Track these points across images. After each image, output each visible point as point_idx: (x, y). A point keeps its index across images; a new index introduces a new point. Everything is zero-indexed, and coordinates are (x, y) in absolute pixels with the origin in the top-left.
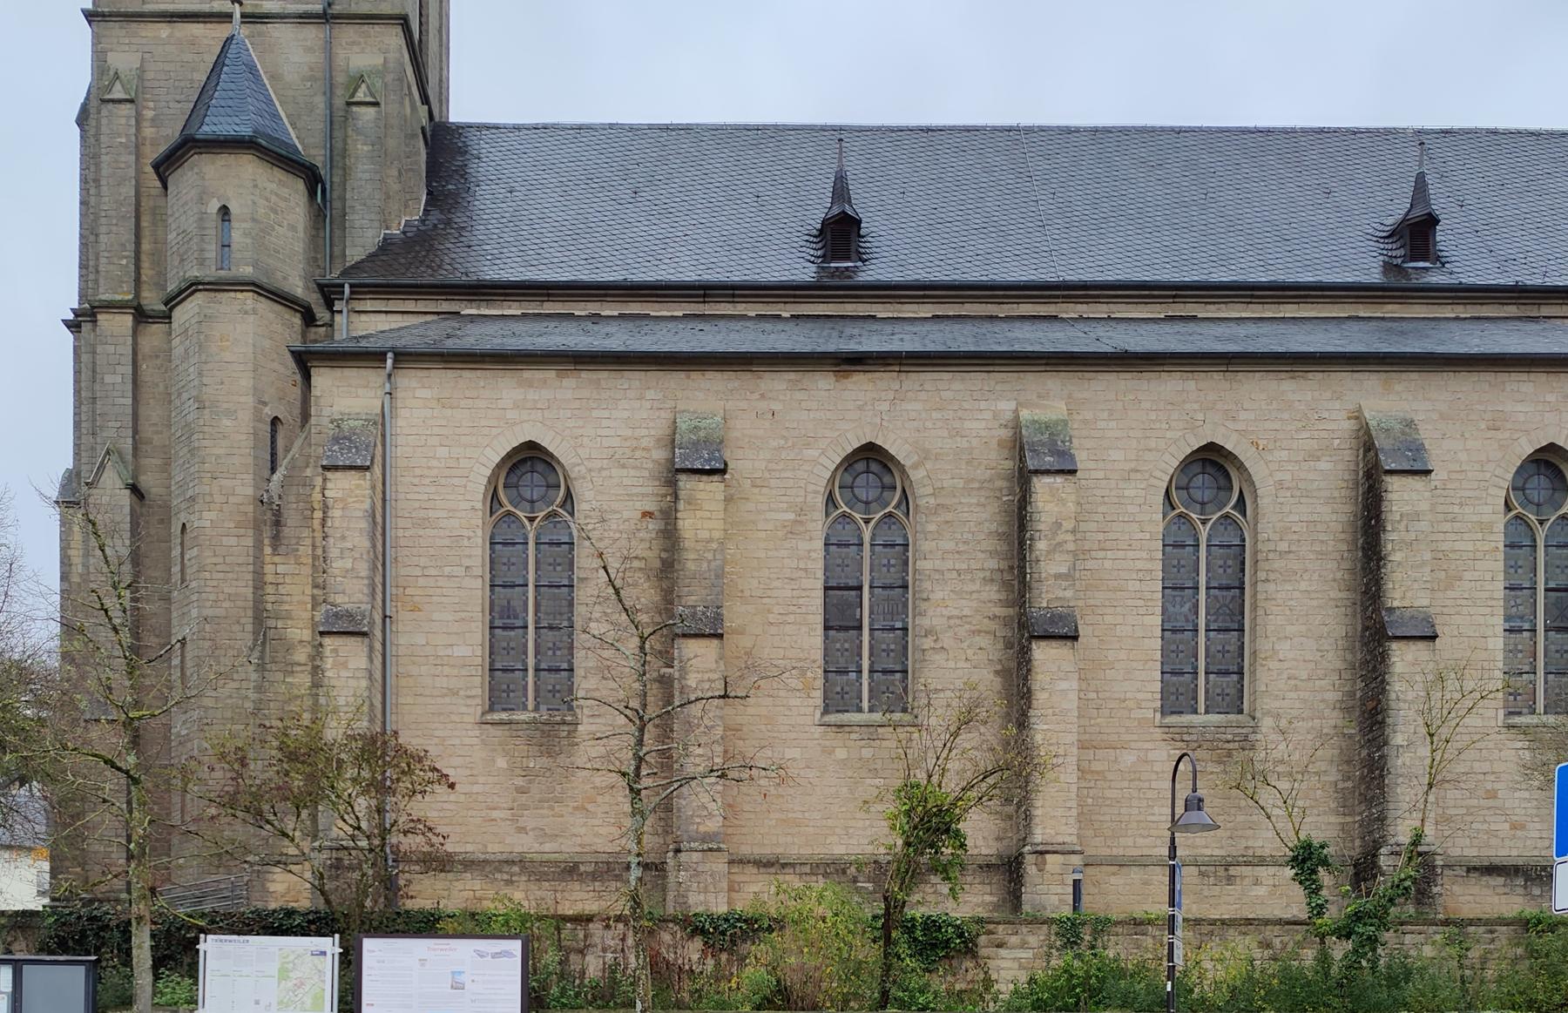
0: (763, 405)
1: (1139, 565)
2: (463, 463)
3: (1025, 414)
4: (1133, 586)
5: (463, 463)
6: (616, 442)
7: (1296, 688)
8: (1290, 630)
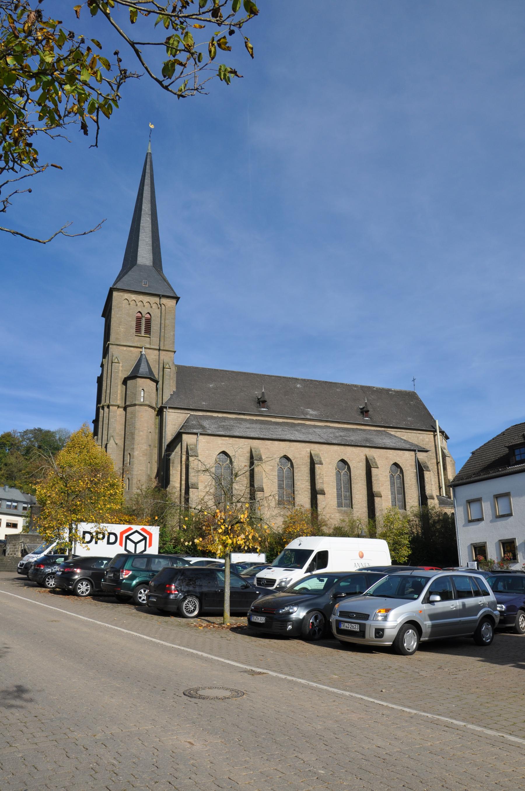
0: (266, 447)
1: (332, 480)
2: (211, 454)
3: (312, 452)
4: (331, 484)
5: (211, 454)
7: (359, 504)
8: (358, 493)
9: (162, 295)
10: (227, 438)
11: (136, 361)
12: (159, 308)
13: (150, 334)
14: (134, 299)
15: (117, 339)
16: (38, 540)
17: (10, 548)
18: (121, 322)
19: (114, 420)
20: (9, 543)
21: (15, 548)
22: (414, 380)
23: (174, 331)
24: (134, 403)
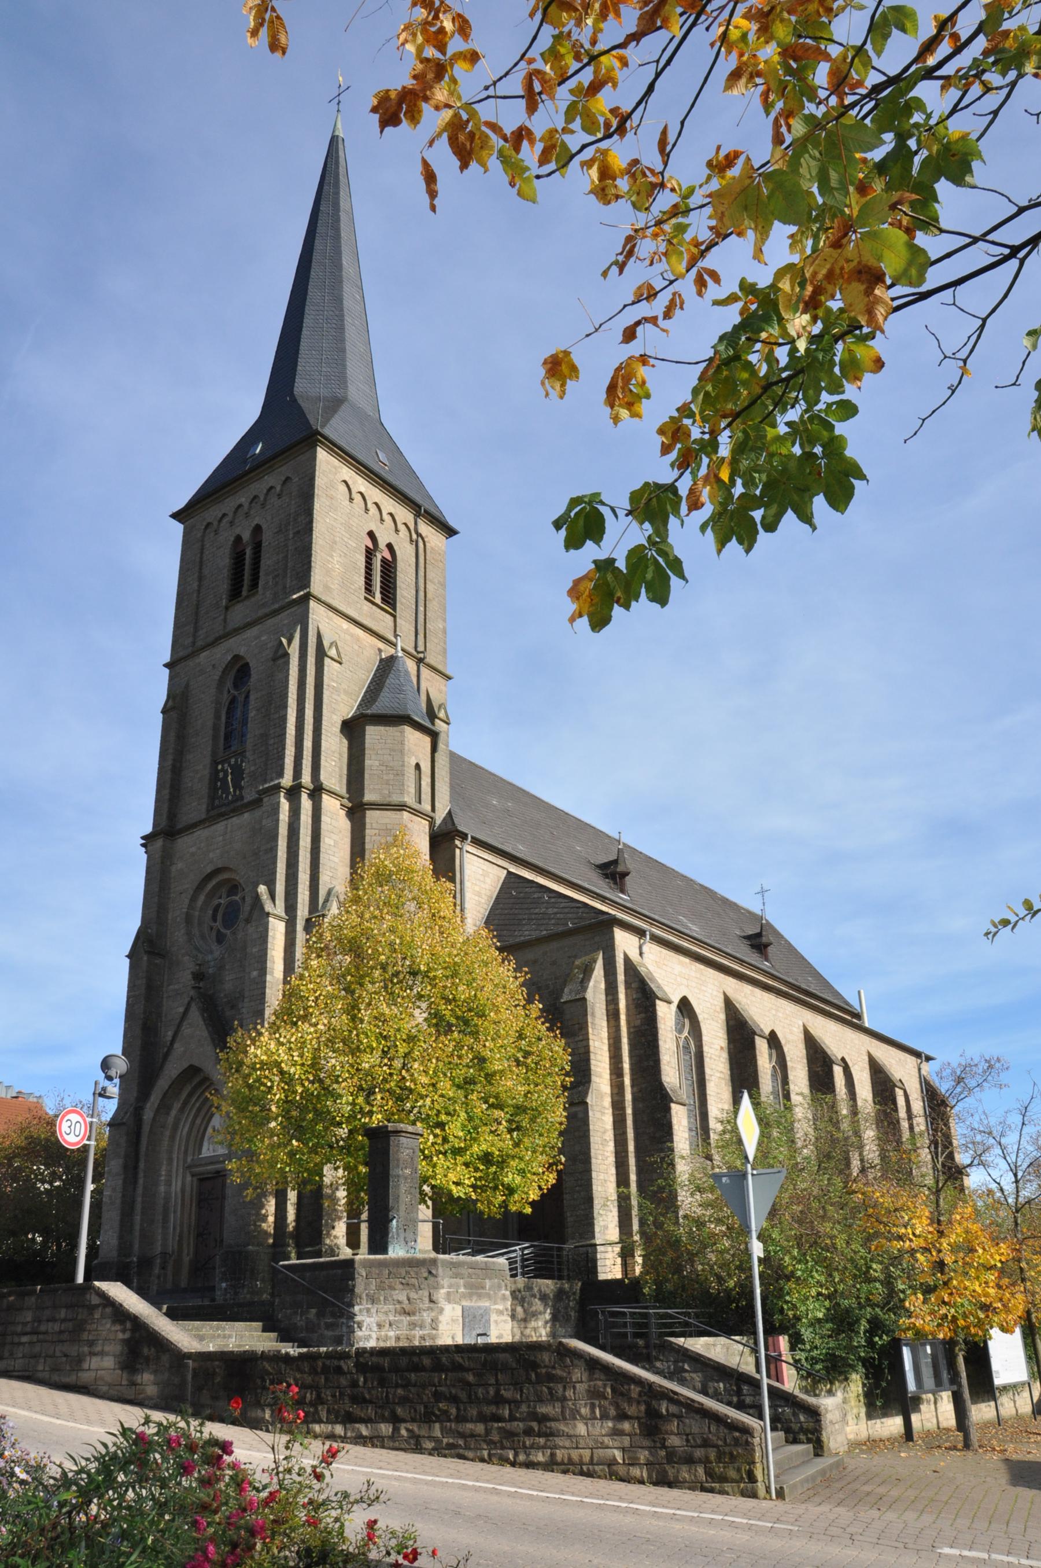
6: (709, 1005)
9: (425, 511)
10: (686, 960)
11: (369, 672)
12: (411, 540)
13: (394, 607)
14: (363, 490)
15: (327, 587)
16: (488, 1283)
17: (380, 1326)
18: (335, 542)
19: (332, 843)
20: (373, 1300)
21: (413, 1325)
22: (763, 892)
23: (444, 620)
24: (395, 799)
